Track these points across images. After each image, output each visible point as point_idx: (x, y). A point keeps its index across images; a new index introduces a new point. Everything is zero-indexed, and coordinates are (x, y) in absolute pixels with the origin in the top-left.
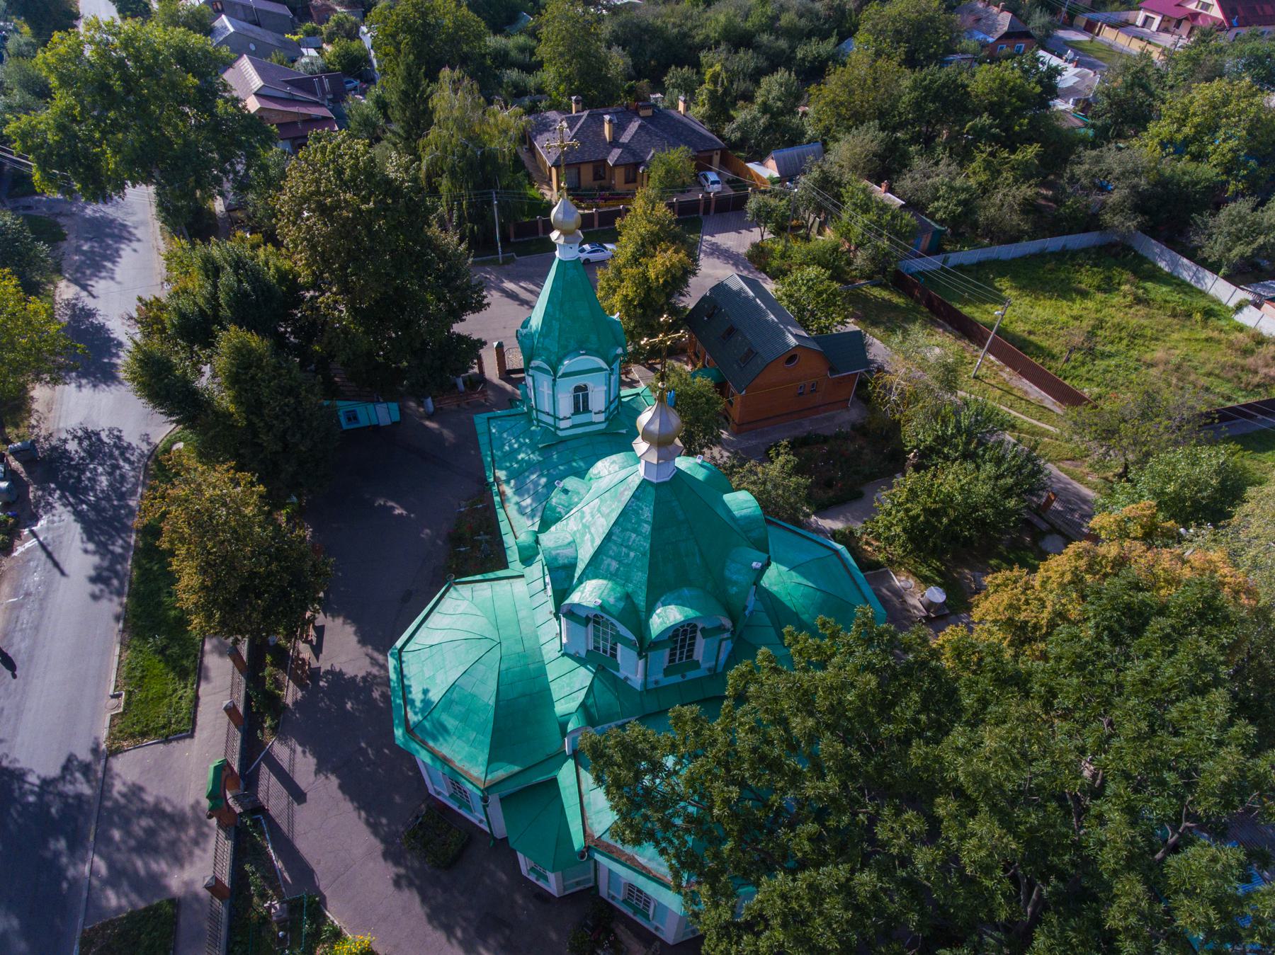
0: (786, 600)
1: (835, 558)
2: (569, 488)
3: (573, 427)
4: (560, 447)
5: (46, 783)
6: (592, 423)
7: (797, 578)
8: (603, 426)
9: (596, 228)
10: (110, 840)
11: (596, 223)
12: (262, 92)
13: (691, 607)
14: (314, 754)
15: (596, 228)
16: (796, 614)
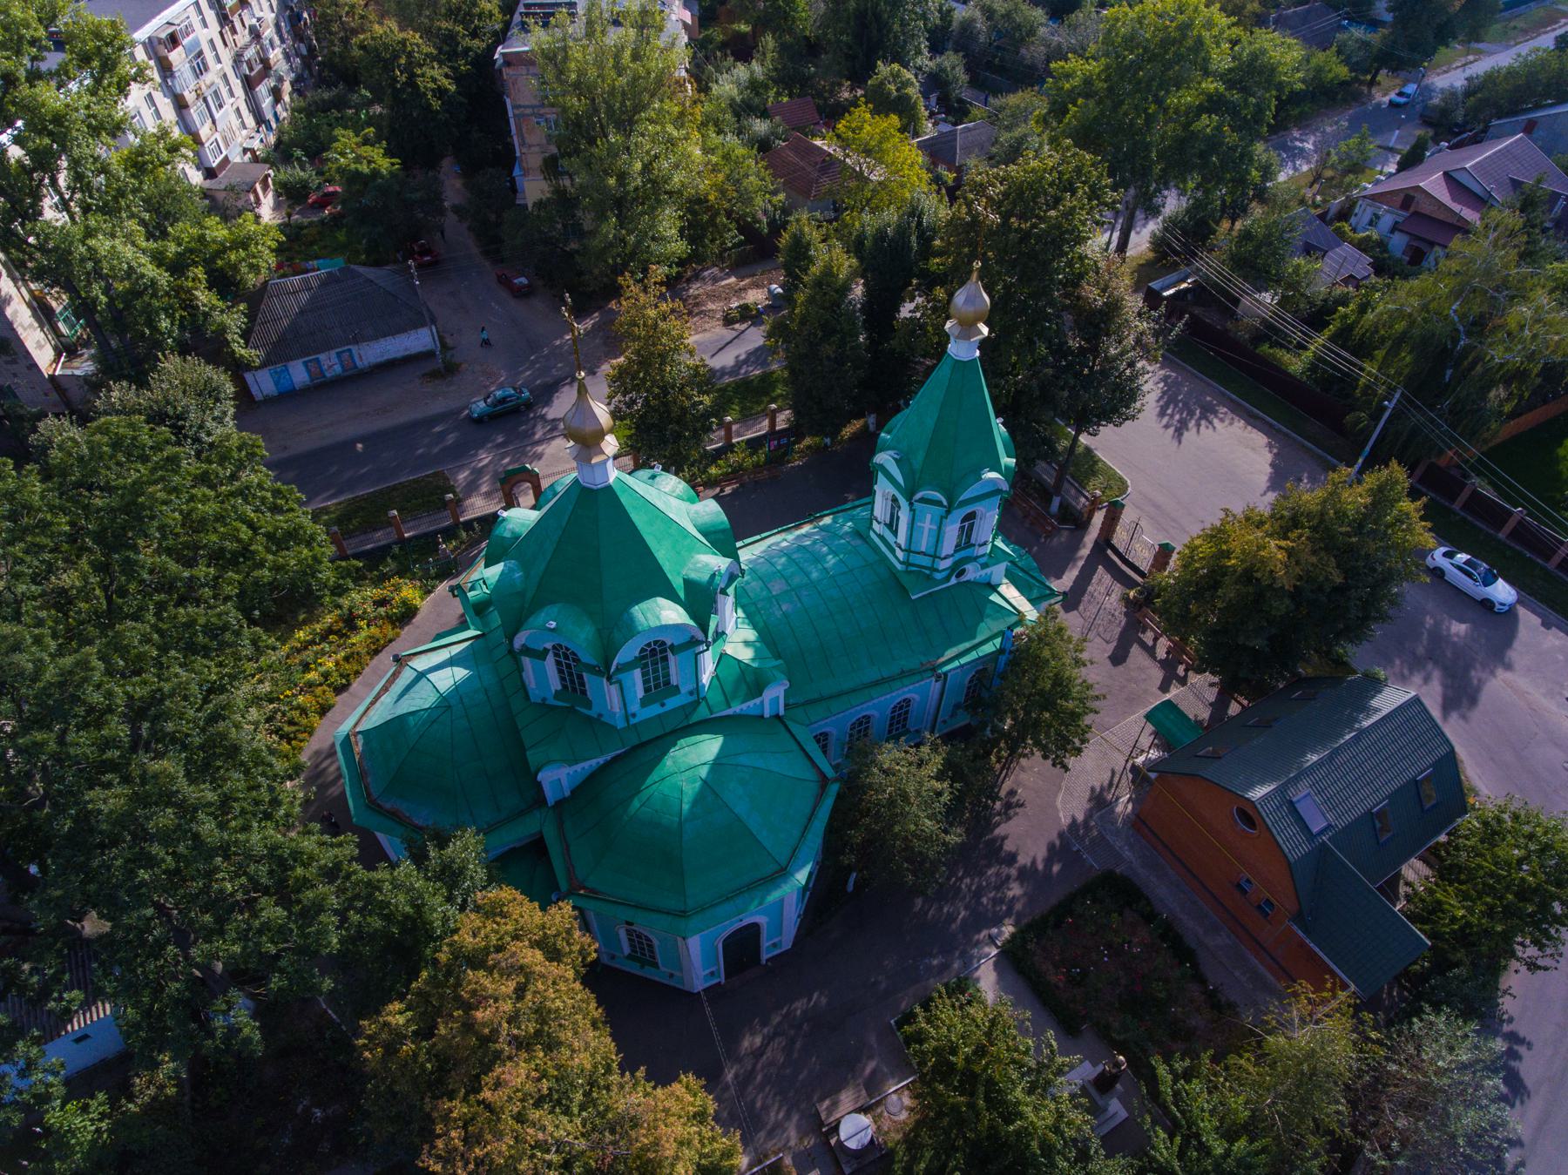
0: (654, 776)
1: (772, 868)
2: (658, 479)
3: (881, 537)
4: (859, 542)
5: (543, 417)
6: (893, 552)
7: (690, 790)
8: (899, 567)
9: (1551, 566)
10: (503, 459)
11: (1556, 560)
12: (1456, 175)
13: (498, 581)
15: (1551, 566)
16: (639, 792)
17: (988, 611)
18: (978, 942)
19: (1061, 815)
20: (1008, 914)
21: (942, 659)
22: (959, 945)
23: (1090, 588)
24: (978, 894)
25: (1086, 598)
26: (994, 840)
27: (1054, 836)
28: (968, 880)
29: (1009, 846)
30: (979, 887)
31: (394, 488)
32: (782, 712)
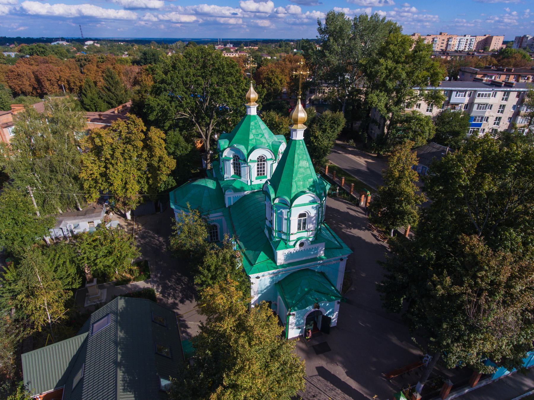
14: (352, 215)
17: (257, 252)
18: (158, 286)
19: (192, 323)
20: (163, 296)
21: (238, 241)
22: (161, 282)
23: (339, 391)
24: (174, 289)
25: (329, 384)
26: (192, 298)
27: (184, 318)
28: (180, 287)
29: (187, 302)
30: (177, 290)
31: (366, 185)
32: (227, 206)
